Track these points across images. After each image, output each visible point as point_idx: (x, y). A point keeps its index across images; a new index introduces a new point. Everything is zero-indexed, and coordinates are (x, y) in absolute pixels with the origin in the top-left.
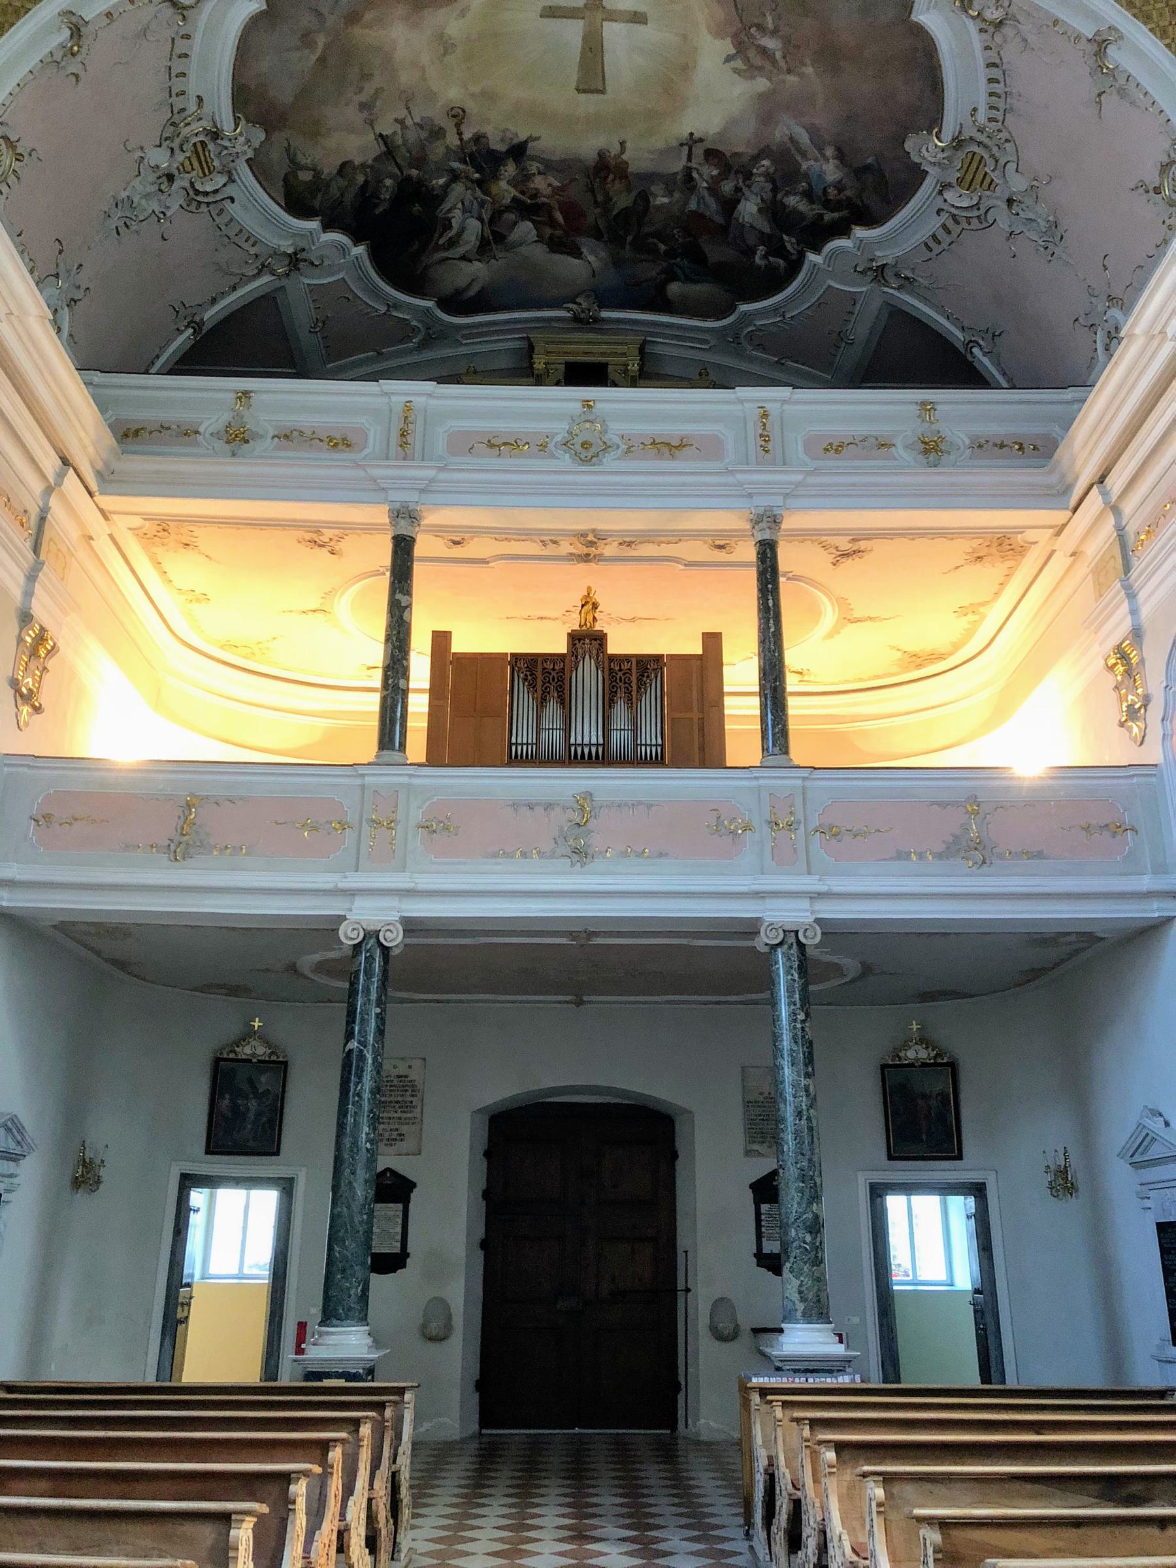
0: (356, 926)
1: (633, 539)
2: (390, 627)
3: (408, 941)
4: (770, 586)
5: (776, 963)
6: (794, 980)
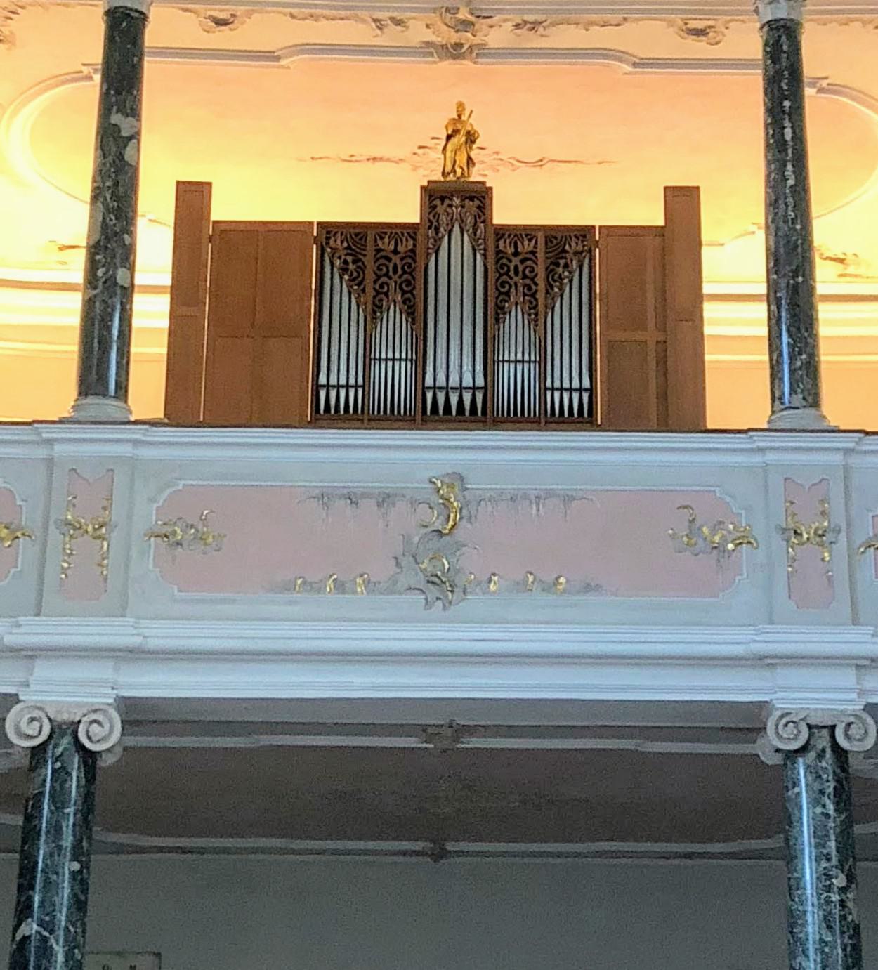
0: (36, 714)
1: (539, 18)
2: (101, 173)
3: (131, 741)
4: (787, 104)
5: (796, 784)
6: (827, 816)
